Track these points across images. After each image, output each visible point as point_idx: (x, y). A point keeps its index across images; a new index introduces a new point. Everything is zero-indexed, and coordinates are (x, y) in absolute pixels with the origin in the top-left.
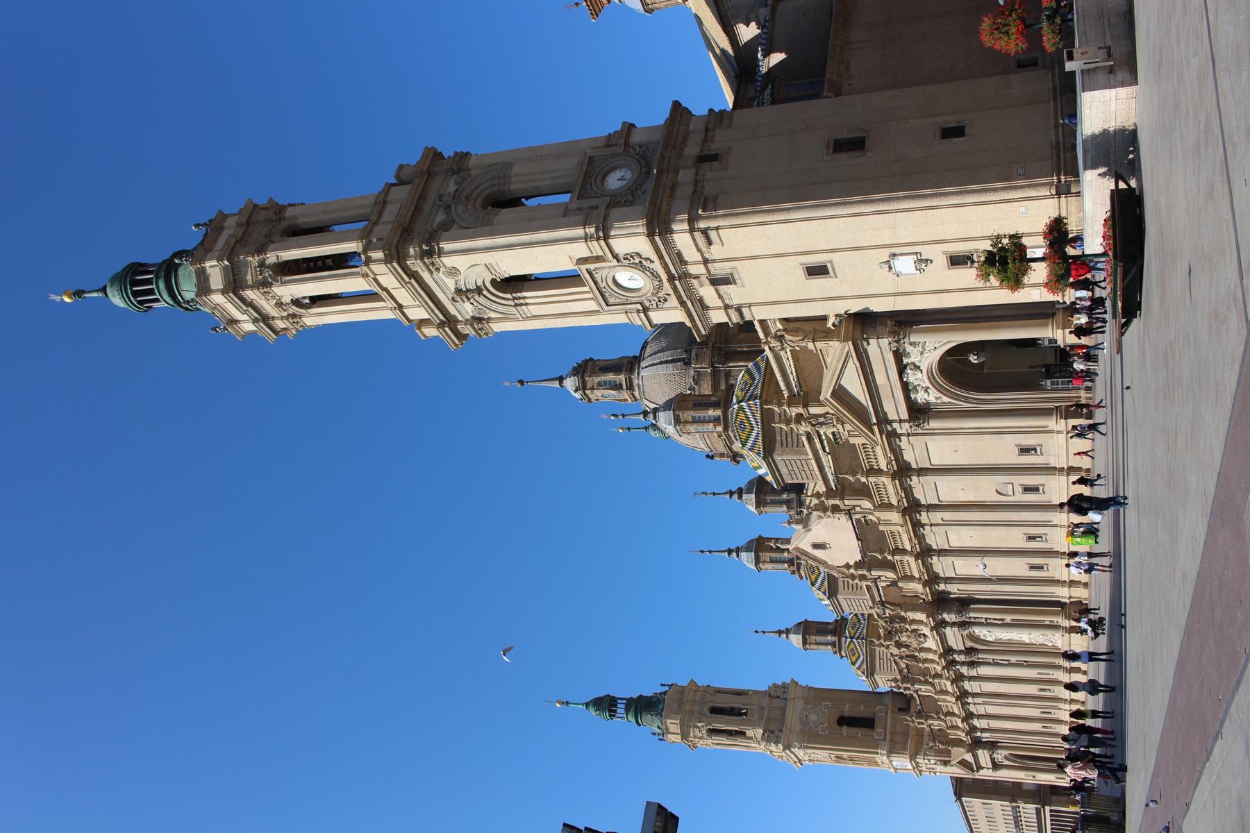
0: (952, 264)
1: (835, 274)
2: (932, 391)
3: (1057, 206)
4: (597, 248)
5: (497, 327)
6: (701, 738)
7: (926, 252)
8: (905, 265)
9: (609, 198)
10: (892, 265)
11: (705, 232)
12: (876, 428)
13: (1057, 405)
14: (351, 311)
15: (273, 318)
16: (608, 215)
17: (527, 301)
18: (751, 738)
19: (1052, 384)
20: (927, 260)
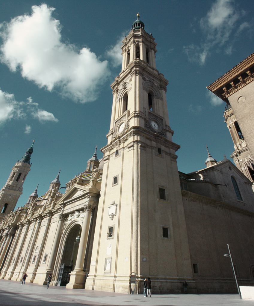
0: (110, 228)
1: (114, 186)
2: (70, 221)
3: (126, 276)
4: (132, 115)
5: (115, 96)
6: (14, 170)
7: (116, 218)
8: (113, 210)
9: (148, 120)
10: (113, 205)
11: (133, 146)
12: (62, 202)
13: (54, 270)
14: (125, 62)
15: (126, 47)
16: (143, 118)
17: (121, 102)
18: (10, 182)
19: (62, 269)
20: (113, 218)
